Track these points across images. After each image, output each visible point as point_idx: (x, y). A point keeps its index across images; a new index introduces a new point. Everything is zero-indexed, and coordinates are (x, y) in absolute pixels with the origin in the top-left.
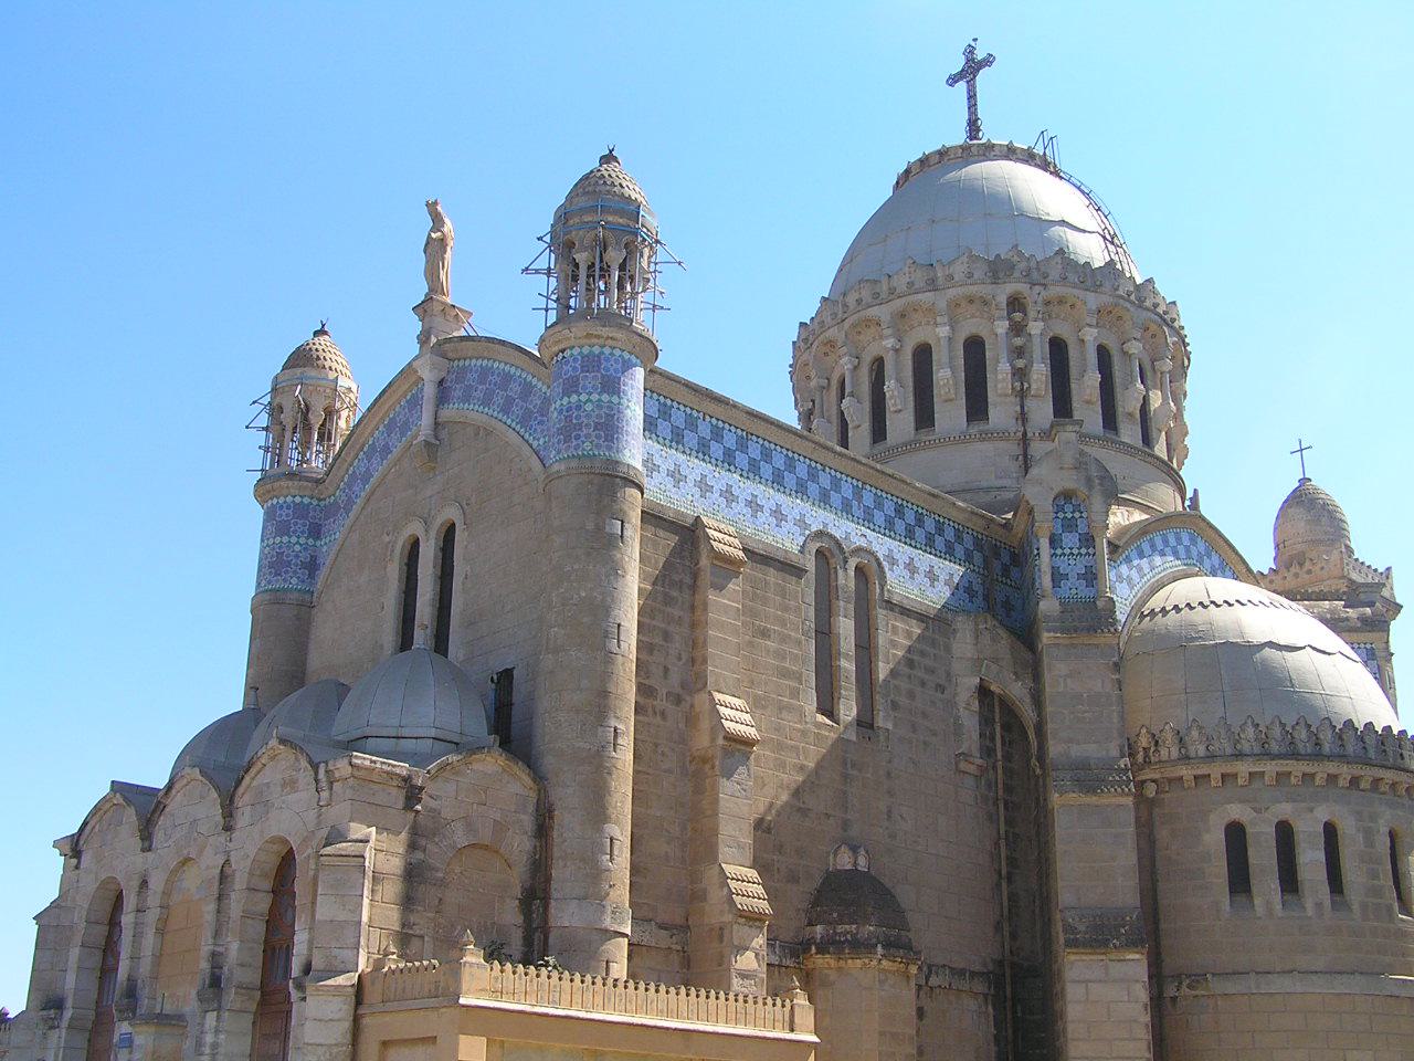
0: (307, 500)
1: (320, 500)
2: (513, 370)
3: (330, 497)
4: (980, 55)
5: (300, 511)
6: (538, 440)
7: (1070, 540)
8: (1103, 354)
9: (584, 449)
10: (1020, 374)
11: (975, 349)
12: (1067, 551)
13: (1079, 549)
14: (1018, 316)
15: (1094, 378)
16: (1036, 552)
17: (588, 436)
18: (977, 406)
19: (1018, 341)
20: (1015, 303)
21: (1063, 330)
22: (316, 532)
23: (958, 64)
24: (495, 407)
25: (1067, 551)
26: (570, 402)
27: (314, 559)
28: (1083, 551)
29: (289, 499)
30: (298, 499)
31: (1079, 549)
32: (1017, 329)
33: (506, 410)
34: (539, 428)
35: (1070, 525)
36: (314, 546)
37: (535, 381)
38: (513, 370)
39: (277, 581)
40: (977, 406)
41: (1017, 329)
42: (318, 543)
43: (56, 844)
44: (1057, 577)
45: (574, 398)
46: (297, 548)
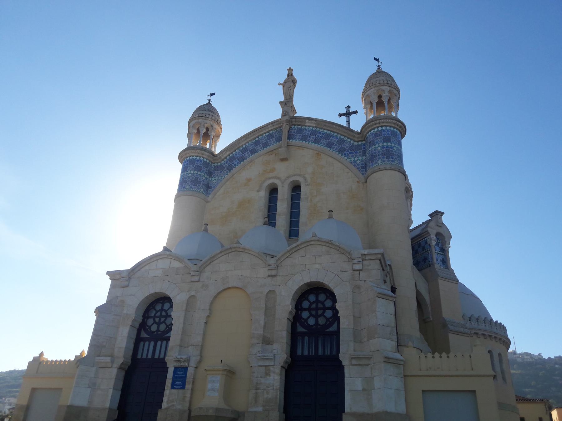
0: (208, 161)
1: (212, 163)
2: (332, 133)
3: (218, 163)
4: (352, 110)
5: (206, 164)
6: (350, 159)
9: (395, 163)
16: (429, 250)
17: (396, 158)
22: (210, 174)
23: (344, 111)
24: (322, 144)
25: (437, 252)
26: (387, 145)
27: (208, 183)
28: (441, 253)
29: (202, 158)
30: (205, 160)
33: (330, 145)
34: (350, 155)
36: (209, 179)
37: (346, 139)
38: (332, 133)
39: (195, 188)
42: (211, 179)
43: (109, 273)
44: (437, 259)
45: (389, 144)
46: (204, 178)
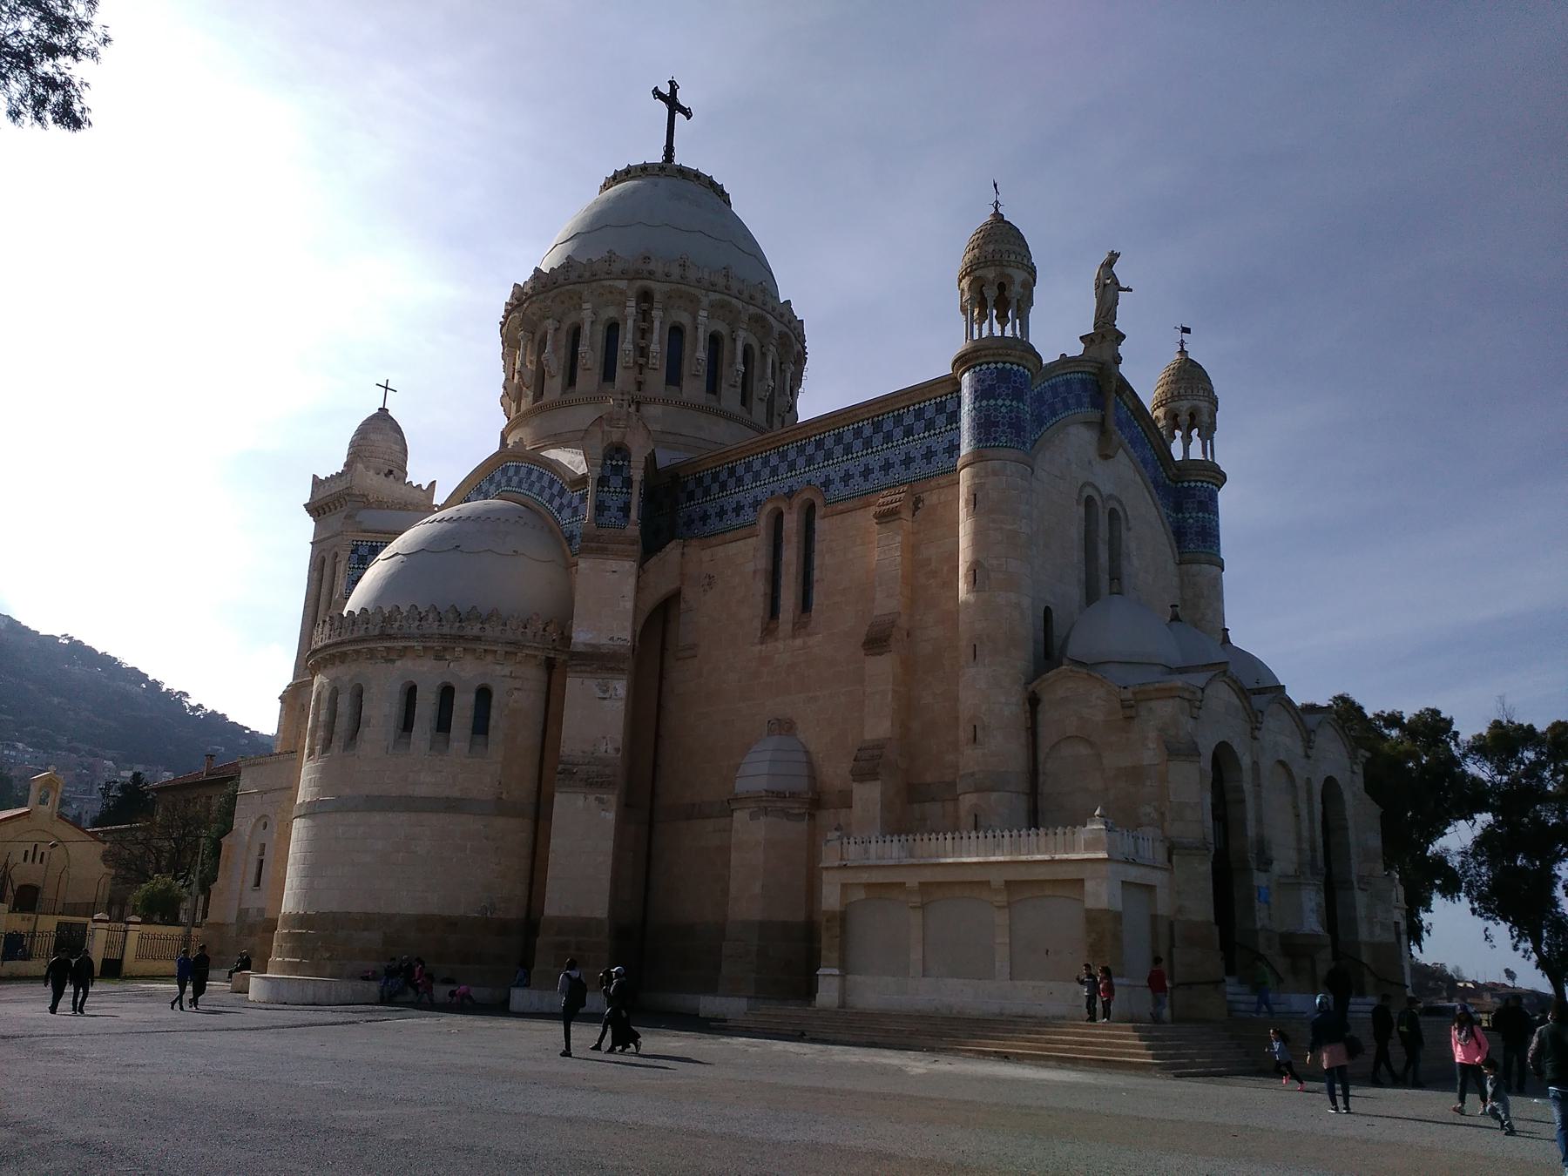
7: (616, 482)
8: (715, 340)
10: (643, 351)
11: (613, 329)
12: (612, 490)
13: (621, 488)
14: (645, 306)
15: (702, 354)
18: (608, 374)
19: (644, 325)
20: (645, 297)
21: (684, 318)
25: (612, 490)
28: (625, 490)
31: (621, 488)
32: (645, 315)
35: (617, 470)
40: (608, 374)
41: (645, 315)
